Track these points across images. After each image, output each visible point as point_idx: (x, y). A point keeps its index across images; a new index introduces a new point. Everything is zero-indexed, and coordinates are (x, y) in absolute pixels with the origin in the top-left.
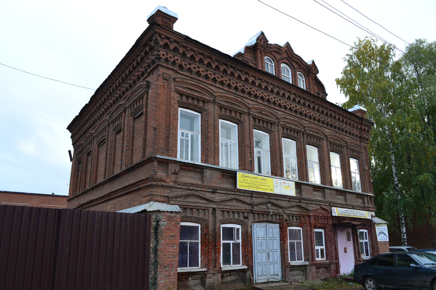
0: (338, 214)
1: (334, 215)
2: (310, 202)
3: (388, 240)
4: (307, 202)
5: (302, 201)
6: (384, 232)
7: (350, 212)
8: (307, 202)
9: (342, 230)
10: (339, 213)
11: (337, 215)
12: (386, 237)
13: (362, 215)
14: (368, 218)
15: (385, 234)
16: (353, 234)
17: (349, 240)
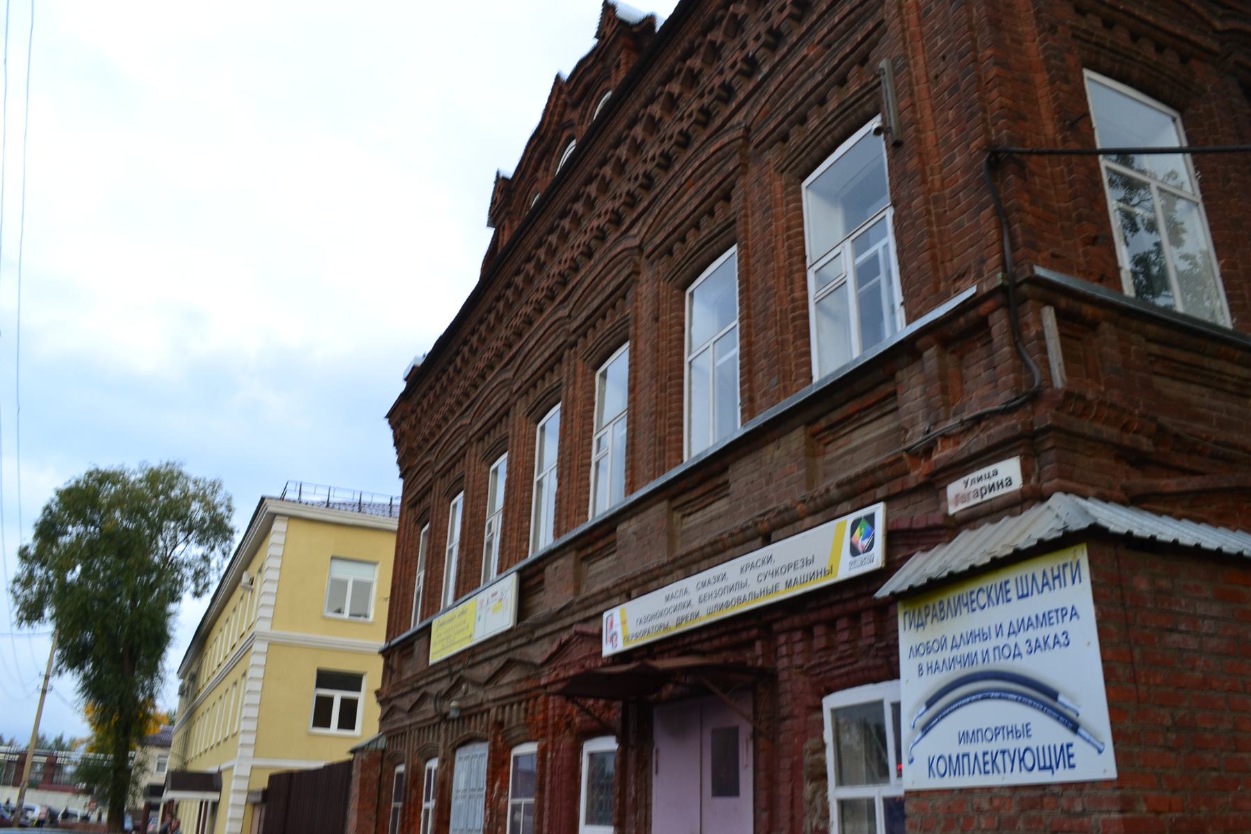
0: (626, 639)
1: (608, 650)
2: (558, 625)
3: (1096, 762)
4: (549, 629)
5: (538, 633)
6: (1031, 666)
7: (694, 596)
8: (549, 629)
9: (679, 731)
10: (633, 628)
11: (621, 647)
12: (1048, 732)
13: (781, 580)
14: (847, 568)
15: (1043, 696)
16: (755, 735)
17: (725, 786)
